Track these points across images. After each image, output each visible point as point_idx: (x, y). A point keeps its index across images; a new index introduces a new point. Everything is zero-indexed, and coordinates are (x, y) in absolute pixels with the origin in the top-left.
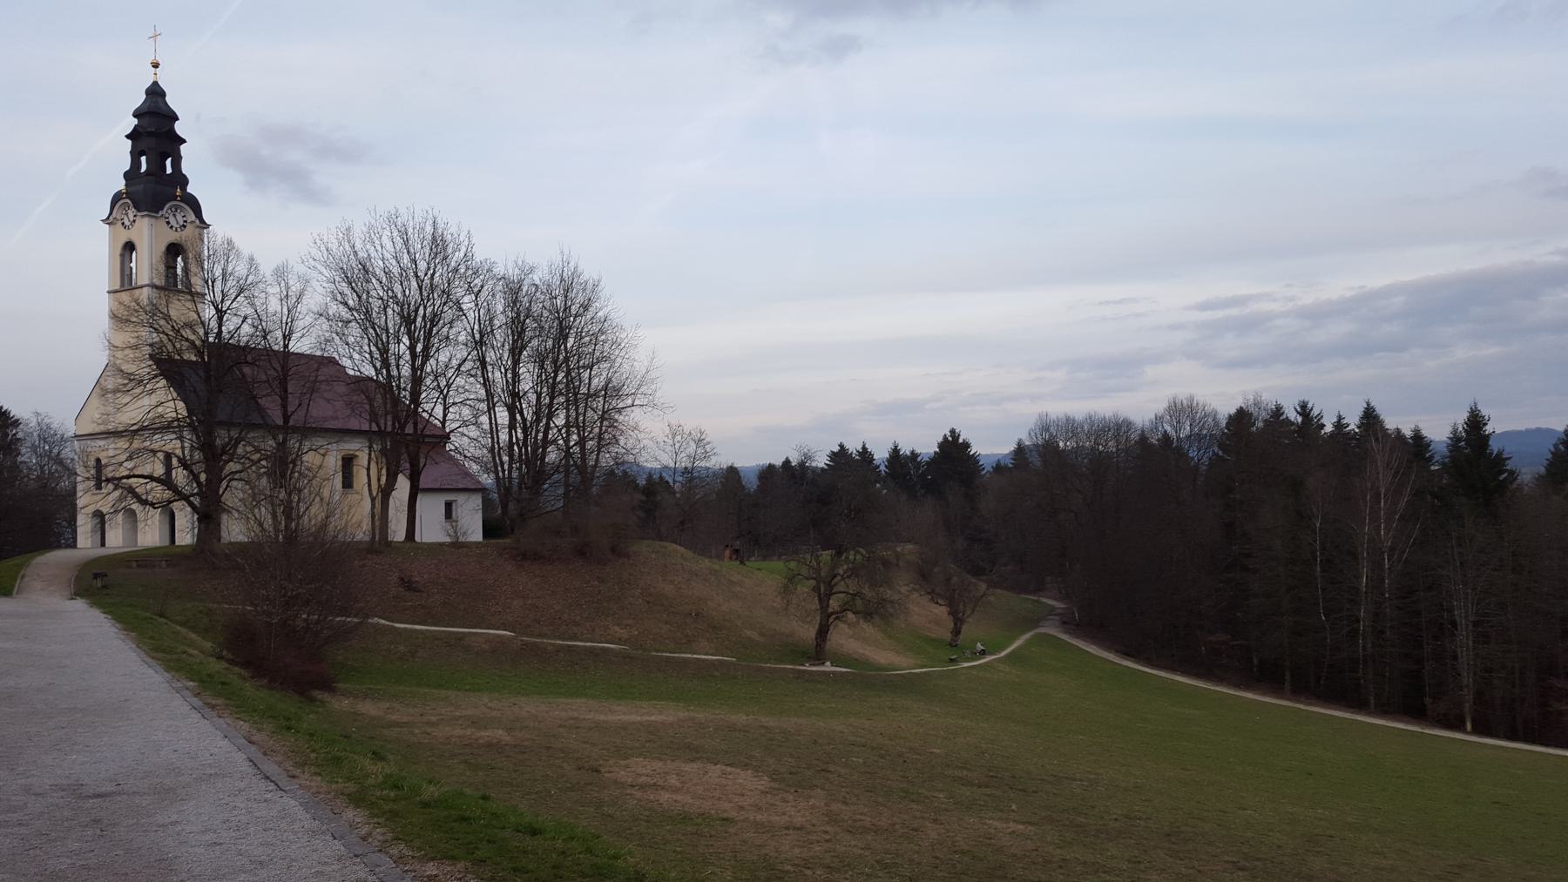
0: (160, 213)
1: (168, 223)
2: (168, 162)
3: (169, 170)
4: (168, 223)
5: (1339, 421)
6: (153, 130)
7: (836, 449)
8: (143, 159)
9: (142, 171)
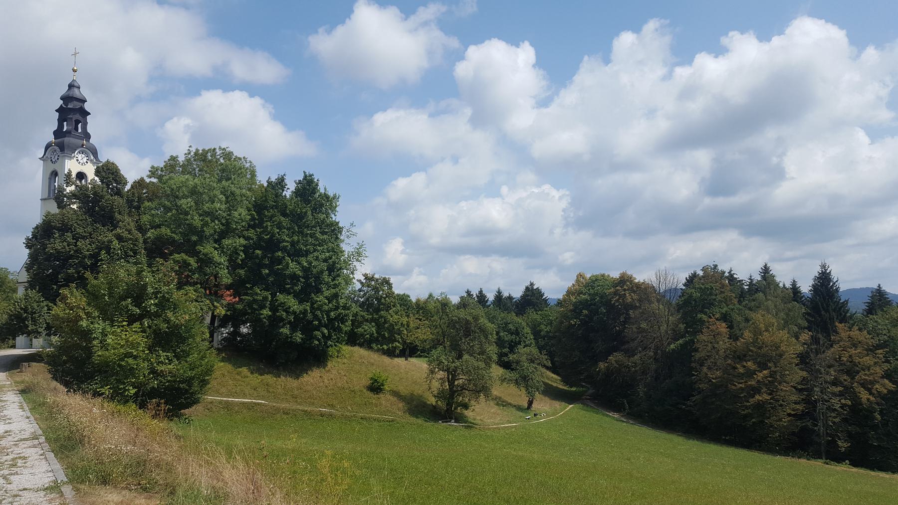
0: (73, 155)
1: (77, 160)
2: (80, 125)
4: (77, 160)
8: (65, 123)
9: (64, 130)
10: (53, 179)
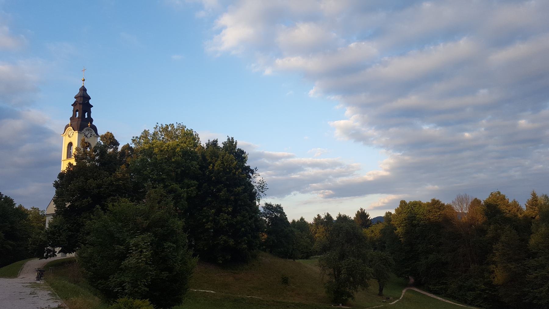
0: (82, 132)
2: (86, 114)
3: (86, 117)
4: (85, 135)
6: (81, 102)
7: (316, 217)
8: (77, 113)
9: (77, 117)
10: (69, 148)
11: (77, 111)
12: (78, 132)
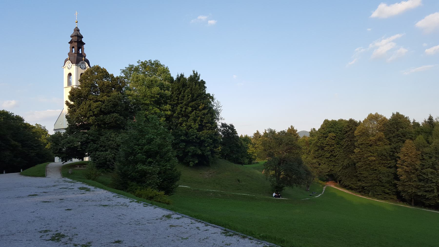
0: (79, 64)
2: (80, 50)
4: (81, 67)
5: (414, 121)
6: (76, 40)
8: (73, 49)
11: (73, 47)
12: (76, 65)
